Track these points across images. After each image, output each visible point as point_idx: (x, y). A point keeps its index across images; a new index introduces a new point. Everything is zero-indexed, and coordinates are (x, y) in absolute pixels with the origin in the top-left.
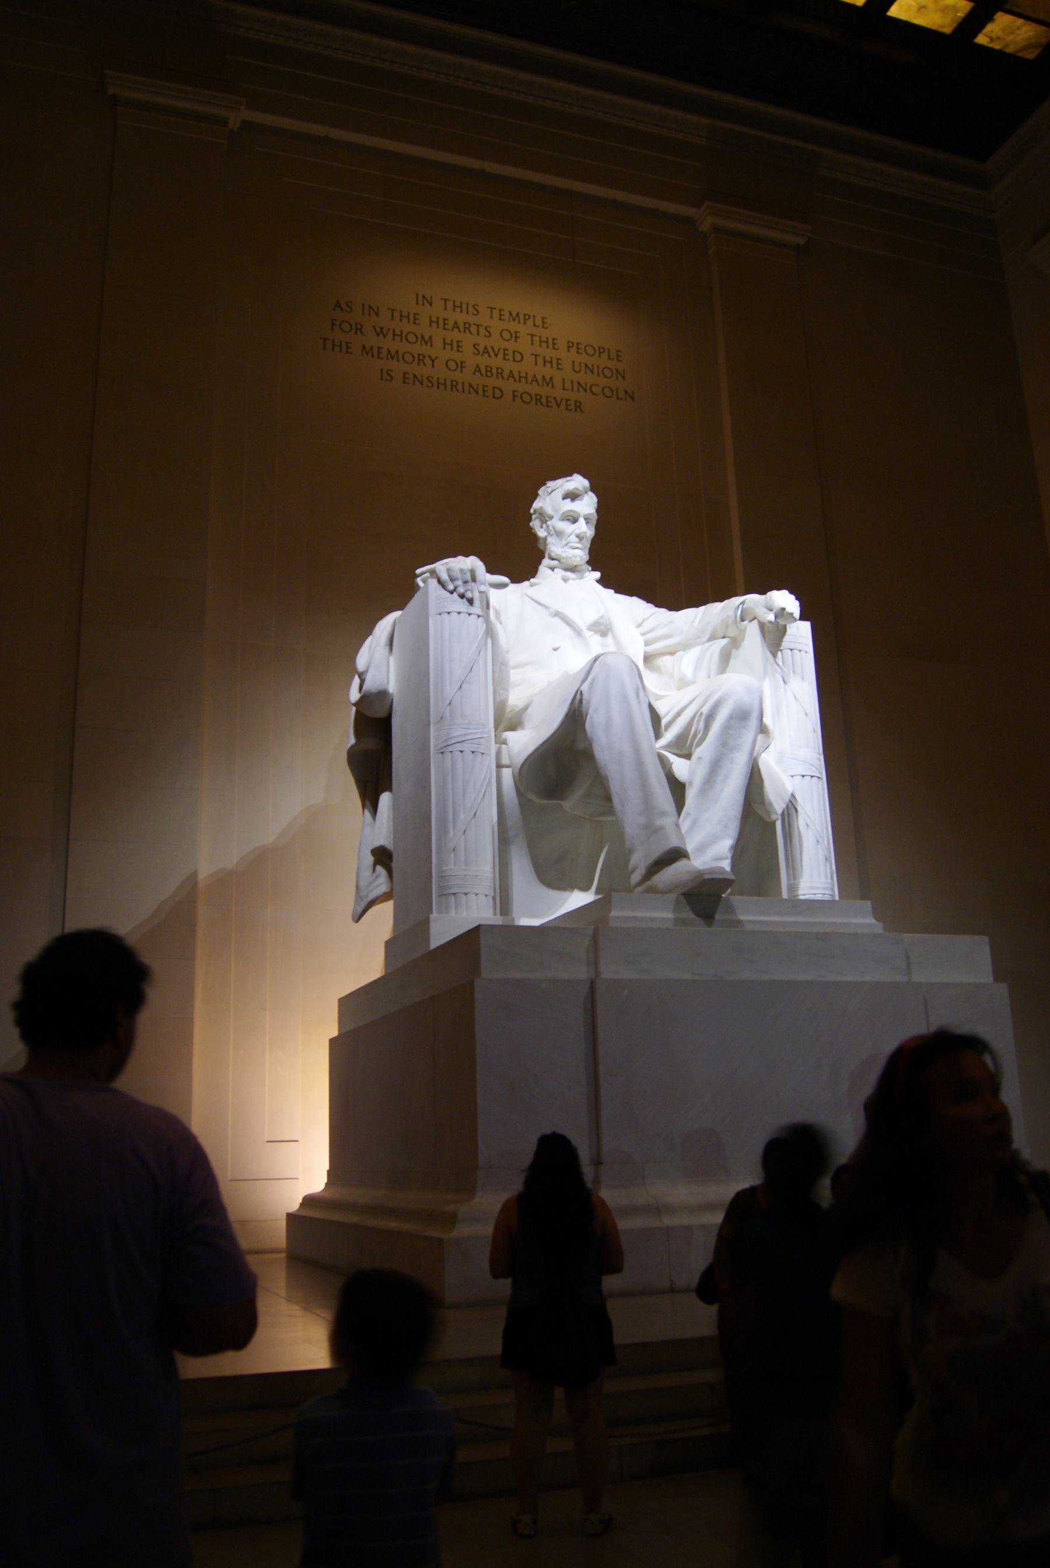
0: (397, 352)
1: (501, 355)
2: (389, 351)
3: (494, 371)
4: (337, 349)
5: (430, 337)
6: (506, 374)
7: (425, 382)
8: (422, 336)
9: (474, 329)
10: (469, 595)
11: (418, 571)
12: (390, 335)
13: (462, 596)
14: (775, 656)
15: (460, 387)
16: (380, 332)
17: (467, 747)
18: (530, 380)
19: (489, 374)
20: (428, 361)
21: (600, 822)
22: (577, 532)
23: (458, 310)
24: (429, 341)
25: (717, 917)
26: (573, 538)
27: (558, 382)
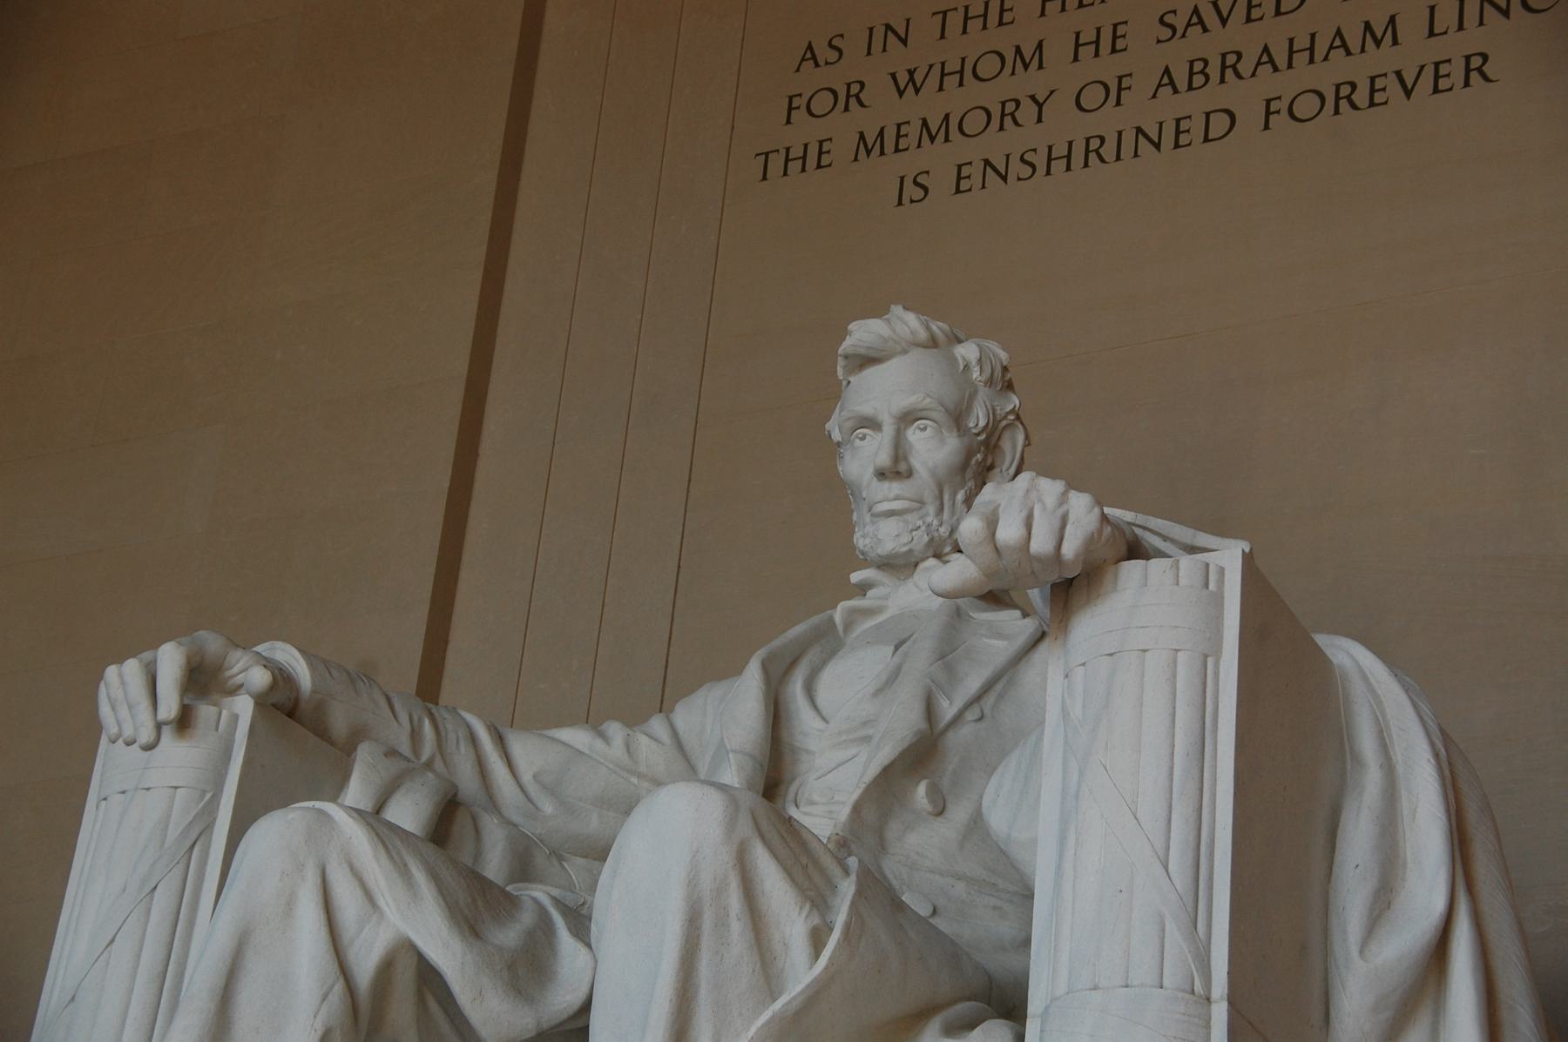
0: (947, 117)
2: (925, 123)
3: (1214, 71)
4: (795, 166)
5: (1040, 45)
6: (1245, 68)
7: (1017, 168)
8: (1018, 50)
15: (1108, 151)
18: (1319, 56)
19: (1198, 80)
20: (1027, 112)
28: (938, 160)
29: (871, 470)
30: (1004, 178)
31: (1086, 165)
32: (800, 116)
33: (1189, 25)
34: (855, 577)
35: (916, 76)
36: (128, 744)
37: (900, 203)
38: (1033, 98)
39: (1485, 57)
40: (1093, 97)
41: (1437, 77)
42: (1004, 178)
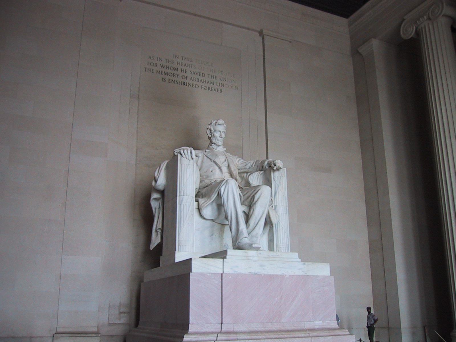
1: (198, 75)
6: (199, 81)
7: (176, 82)
8: (175, 68)
9: (191, 66)
11: (175, 150)
12: (165, 67)
15: (186, 84)
16: (162, 66)
18: (207, 82)
19: (195, 80)
22: (220, 136)
23: (186, 60)
24: (177, 70)
27: (215, 84)
28: (167, 78)
29: (218, 136)
30: (174, 83)
31: (183, 85)
32: (149, 65)
33: (193, 73)
34: (213, 145)
35: (164, 66)
36: (187, 159)
37: (162, 81)
38: (177, 74)
39: (222, 90)
40: (184, 77)
41: (218, 90)
42: (174, 83)
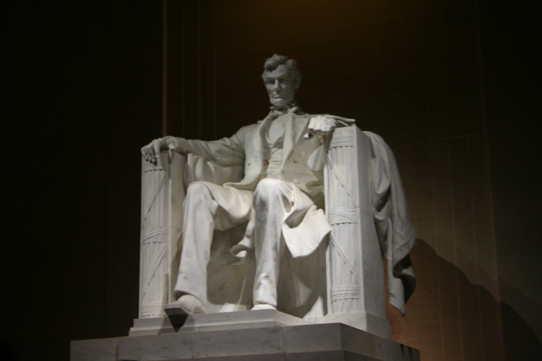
10: (153, 160)
13: (151, 162)
14: (327, 152)
17: (151, 241)
21: (236, 266)
25: (185, 326)
26: (275, 93)
34: (272, 108)
